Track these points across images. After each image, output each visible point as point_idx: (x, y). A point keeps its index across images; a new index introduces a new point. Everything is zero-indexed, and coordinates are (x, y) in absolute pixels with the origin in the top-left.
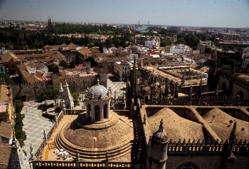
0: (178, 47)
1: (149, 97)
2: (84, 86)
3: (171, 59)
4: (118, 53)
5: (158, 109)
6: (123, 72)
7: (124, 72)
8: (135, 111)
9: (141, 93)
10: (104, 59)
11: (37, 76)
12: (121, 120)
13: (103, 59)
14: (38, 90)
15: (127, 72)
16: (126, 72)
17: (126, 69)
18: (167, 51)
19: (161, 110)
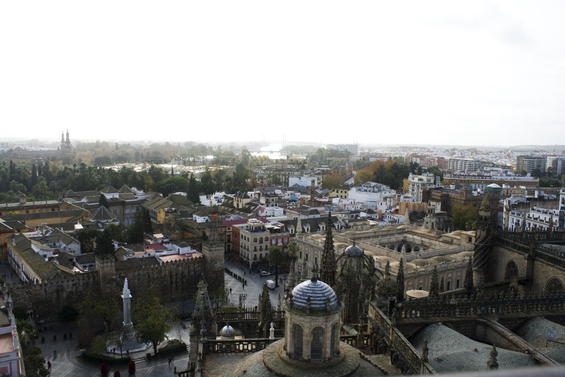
0: (366, 188)
3: (354, 215)
4: (236, 207)
5: (419, 328)
6: (255, 247)
7: (258, 248)
9: (380, 294)
10: (207, 221)
11: (61, 264)
13: (205, 221)
14: (65, 295)
15: (264, 247)
16: (261, 247)
17: (261, 242)
18: (342, 196)
19: (428, 329)
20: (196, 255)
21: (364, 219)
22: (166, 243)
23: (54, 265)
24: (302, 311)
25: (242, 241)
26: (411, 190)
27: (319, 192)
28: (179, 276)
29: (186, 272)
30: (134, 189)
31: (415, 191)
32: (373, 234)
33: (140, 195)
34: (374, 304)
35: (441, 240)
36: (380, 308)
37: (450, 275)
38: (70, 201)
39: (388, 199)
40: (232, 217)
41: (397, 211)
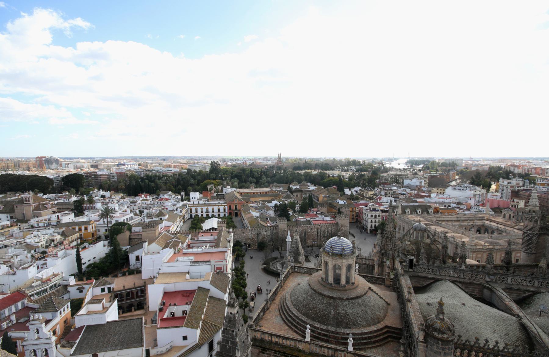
0: (459, 188)
1: (415, 260)
2: (318, 236)
3: (447, 206)
7: (373, 221)
8: (391, 279)
9: (402, 253)
12: (372, 290)
15: (377, 220)
17: (375, 217)
19: (438, 283)
20: (334, 222)
21: (453, 208)
22: (319, 214)
23: (258, 221)
24: (328, 253)
25: (364, 217)
26: (500, 190)
27: (424, 189)
28: (322, 232)
29: (326, 230)
30: (309, 184)
31: (504, 191)
32: (456, 219)
33: (312, 188)
34: (398, 259)
35: (517, 227)
36: (401, 263)
37: (519, 255)
38: (274, 189)
39: (477, 196)
40: (362, 202)
41: (483, 205)
